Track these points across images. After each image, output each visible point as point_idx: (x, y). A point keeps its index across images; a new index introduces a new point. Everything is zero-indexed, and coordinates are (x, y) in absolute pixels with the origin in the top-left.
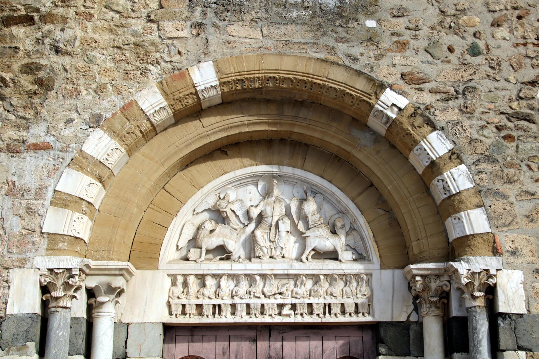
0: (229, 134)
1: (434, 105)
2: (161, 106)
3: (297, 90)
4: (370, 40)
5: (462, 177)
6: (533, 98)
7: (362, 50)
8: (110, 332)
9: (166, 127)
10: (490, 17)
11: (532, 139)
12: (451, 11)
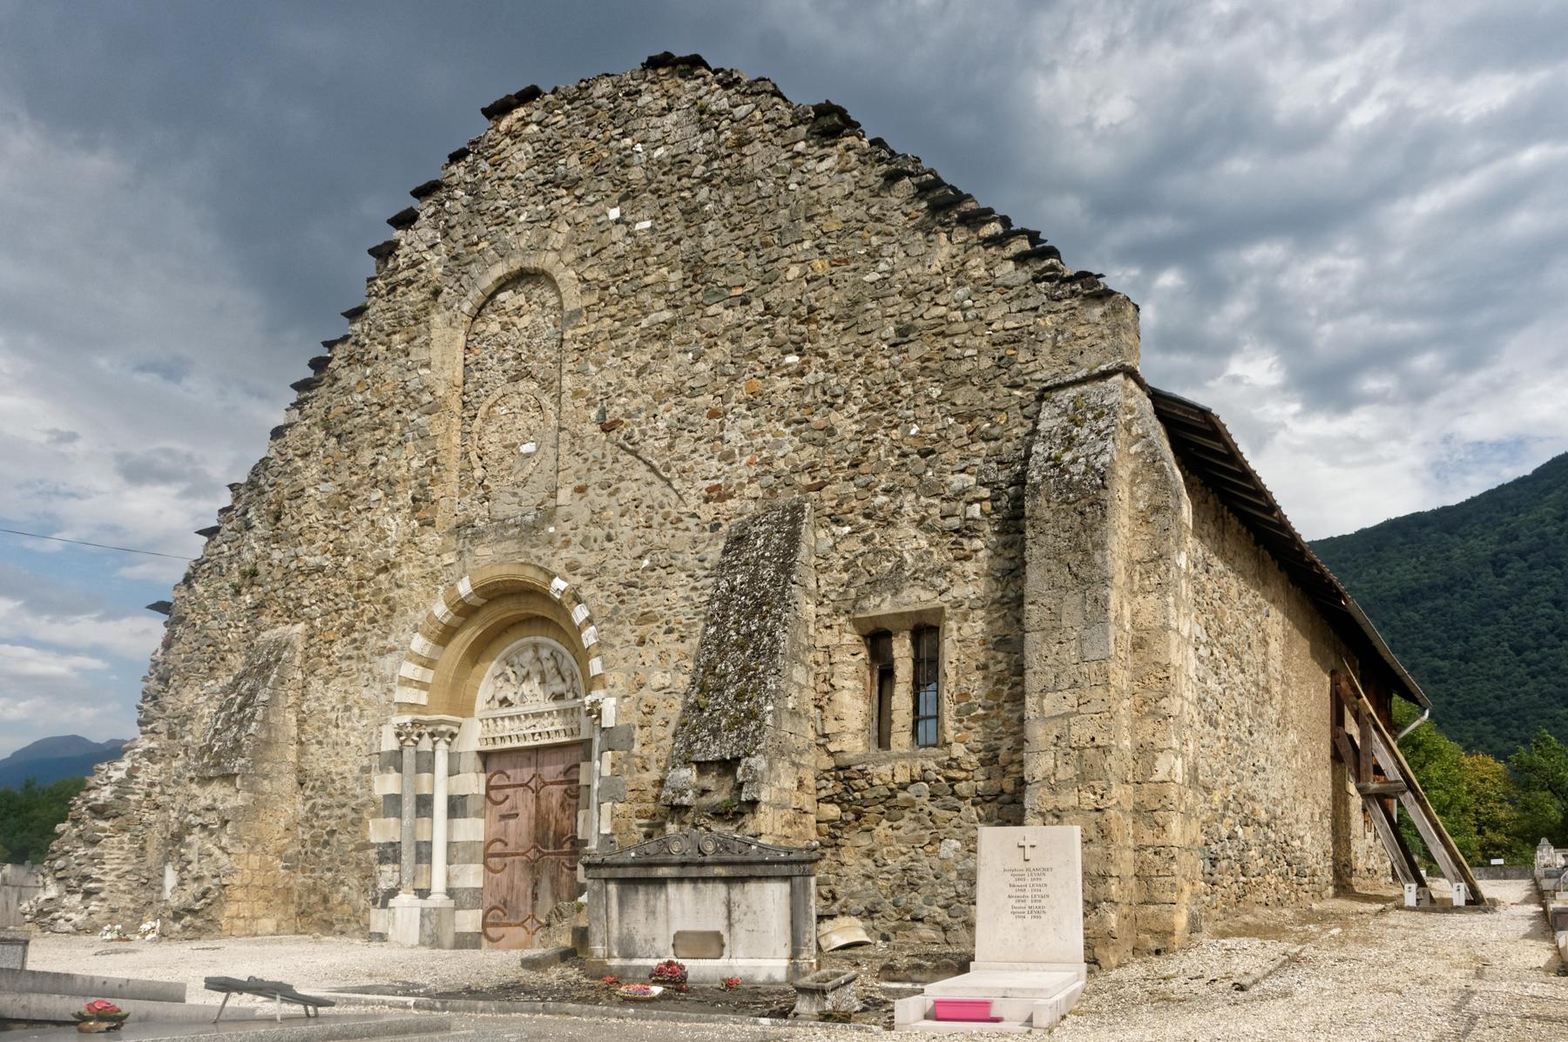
4: (550, 543)
12: (597, 510)
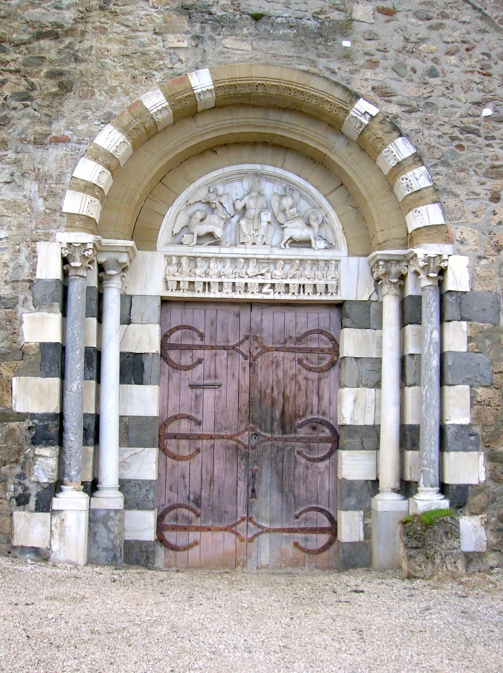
0: (221, 134)
1: (400, 115)
2: (163, 106)
3: (282, 95)
5: (423, 177)
6: (479, 116)
7: (339, 65)
8: (118, 301)
9: (166, 126)
10: (444, 48)
11: (478, 150)
12: (413, 39)
